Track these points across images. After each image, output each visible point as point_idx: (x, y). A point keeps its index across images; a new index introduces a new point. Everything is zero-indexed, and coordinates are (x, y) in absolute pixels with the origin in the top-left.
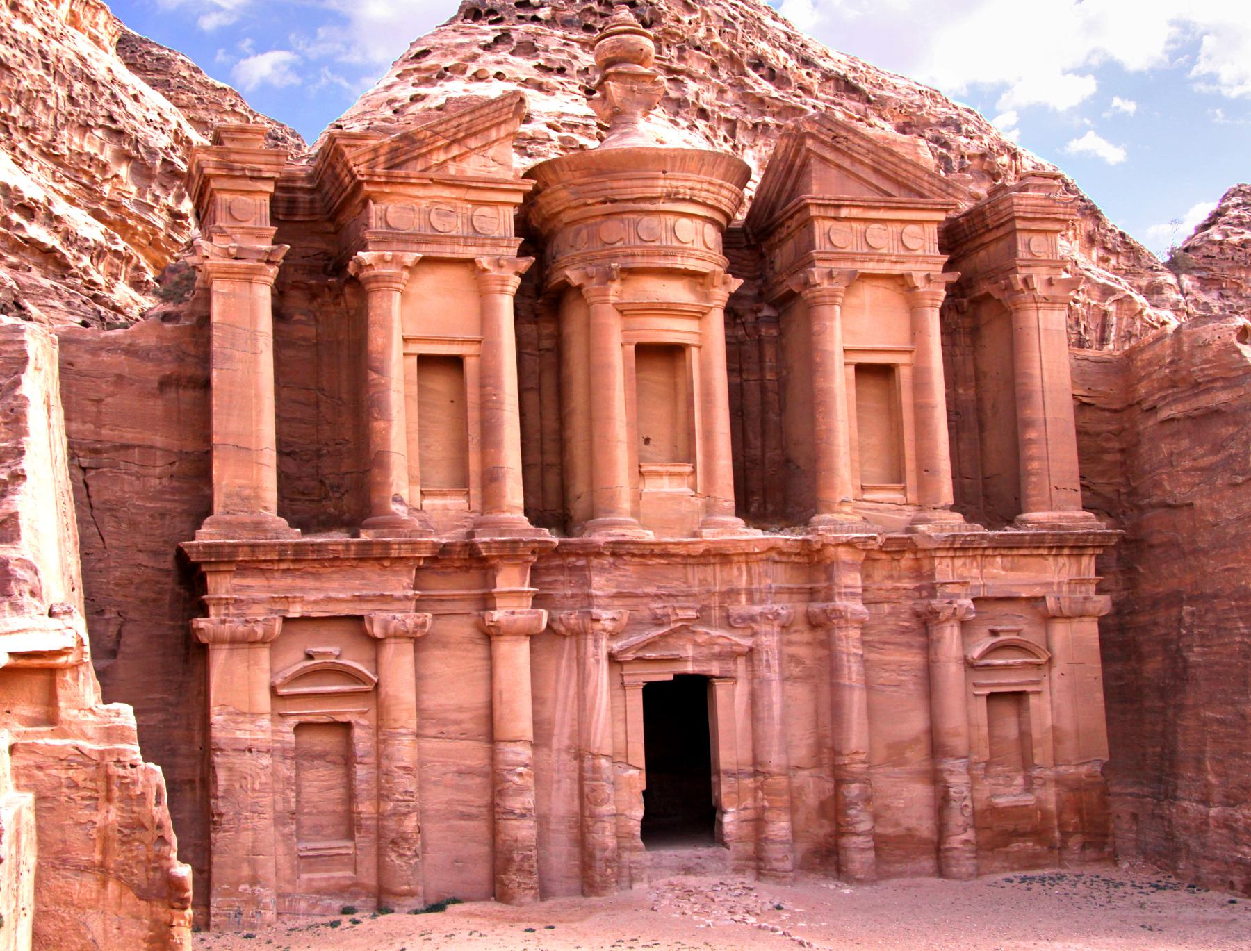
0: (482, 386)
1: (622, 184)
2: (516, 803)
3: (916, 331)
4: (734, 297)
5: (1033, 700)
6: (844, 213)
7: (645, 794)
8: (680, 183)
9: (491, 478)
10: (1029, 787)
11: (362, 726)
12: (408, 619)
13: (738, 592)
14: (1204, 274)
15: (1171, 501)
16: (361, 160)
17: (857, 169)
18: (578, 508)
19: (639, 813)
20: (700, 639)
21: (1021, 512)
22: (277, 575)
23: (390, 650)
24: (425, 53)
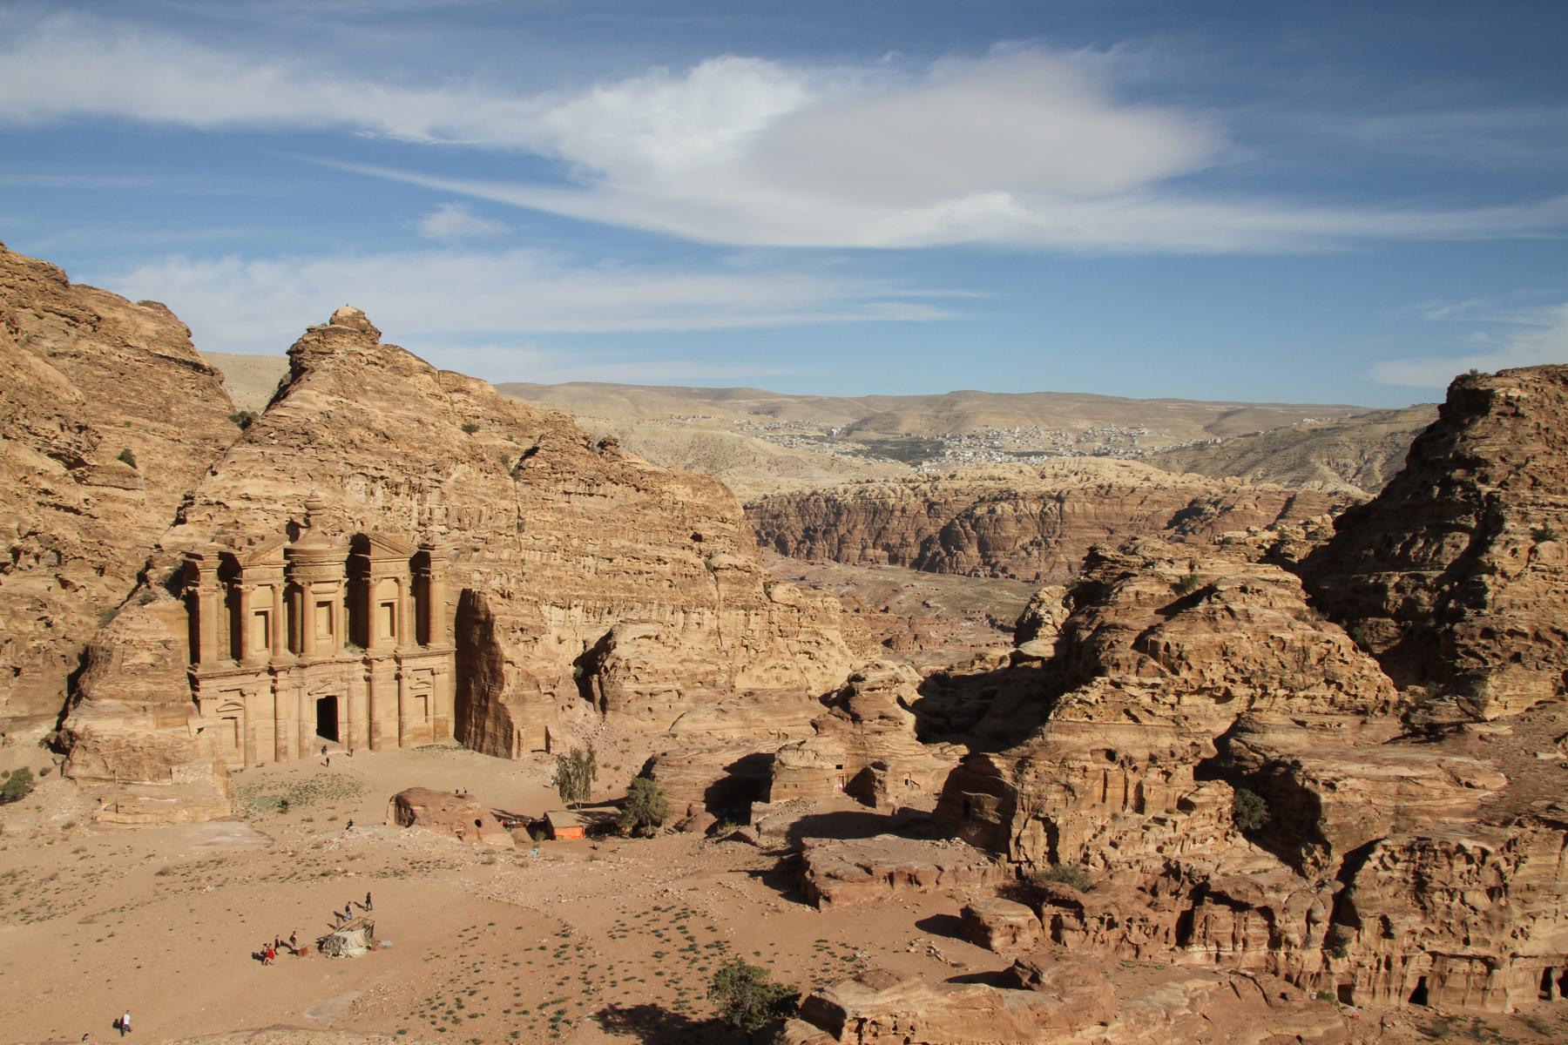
2: (282, 736)
3: (400, 592)
4: (346, 585)
9: (275, 647)
10: (426, 721)
12: (254, 689)
18: (298, 647)
23: (248, 698)
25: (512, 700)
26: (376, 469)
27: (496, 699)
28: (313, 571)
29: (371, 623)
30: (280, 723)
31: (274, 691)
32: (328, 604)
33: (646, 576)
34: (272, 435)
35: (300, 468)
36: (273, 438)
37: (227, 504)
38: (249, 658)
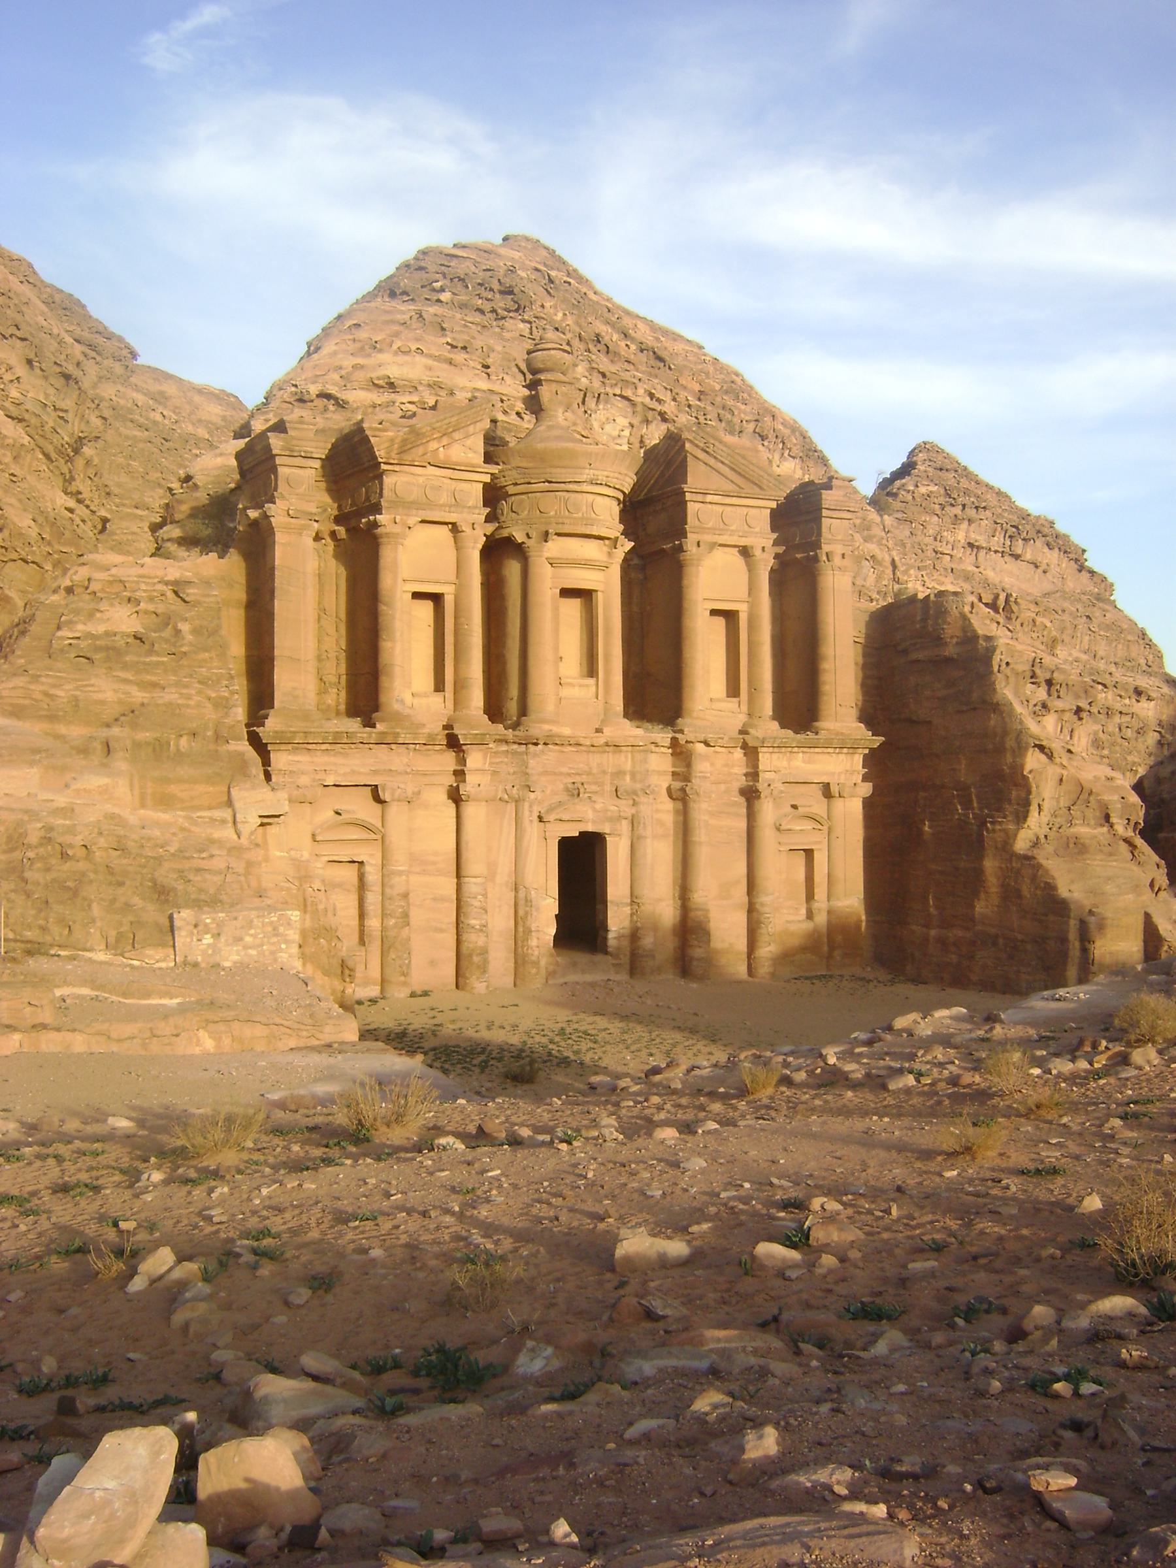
0: (456, 618)
1: (558, 470)
3: (752, 588)
5: (816, 855)
6: (709, 498)
7: (558, 917)
8: (599, 473)
9: (460, 686)
11: (372, 865)
13: (624, 773)
14: (900, 515)
15: (915, 718)
16: (382, 447)
17: (719, 466)
18: (512, 707)
19: (553, 930)
20: (598, 806)
21: (816, 720)
22: (319, 753)
24: (357, 326)
25: (1050, 848)
26: (652, 396)
27: (1005, 847)
28: (552, 506)
29: (687, 654)
30: (472, 886)
31: (455, 797)
32: (585, 595)
33: (1117, 719)
34: (437, 285)
35: (499, 348)
36: (442, 290)
37: (342, 396)
38: (396, 706)
